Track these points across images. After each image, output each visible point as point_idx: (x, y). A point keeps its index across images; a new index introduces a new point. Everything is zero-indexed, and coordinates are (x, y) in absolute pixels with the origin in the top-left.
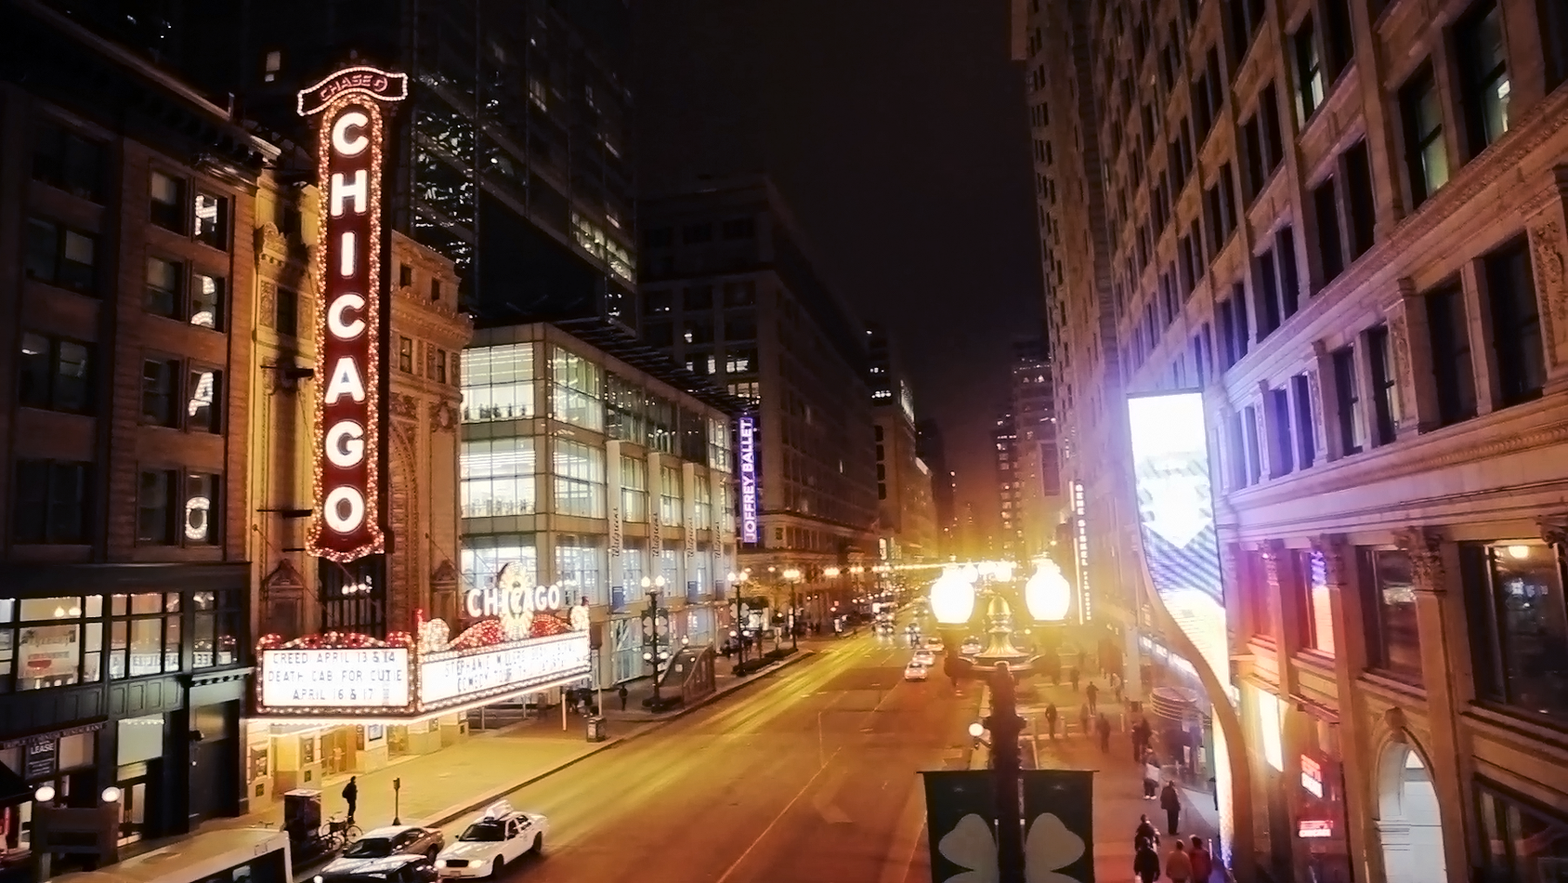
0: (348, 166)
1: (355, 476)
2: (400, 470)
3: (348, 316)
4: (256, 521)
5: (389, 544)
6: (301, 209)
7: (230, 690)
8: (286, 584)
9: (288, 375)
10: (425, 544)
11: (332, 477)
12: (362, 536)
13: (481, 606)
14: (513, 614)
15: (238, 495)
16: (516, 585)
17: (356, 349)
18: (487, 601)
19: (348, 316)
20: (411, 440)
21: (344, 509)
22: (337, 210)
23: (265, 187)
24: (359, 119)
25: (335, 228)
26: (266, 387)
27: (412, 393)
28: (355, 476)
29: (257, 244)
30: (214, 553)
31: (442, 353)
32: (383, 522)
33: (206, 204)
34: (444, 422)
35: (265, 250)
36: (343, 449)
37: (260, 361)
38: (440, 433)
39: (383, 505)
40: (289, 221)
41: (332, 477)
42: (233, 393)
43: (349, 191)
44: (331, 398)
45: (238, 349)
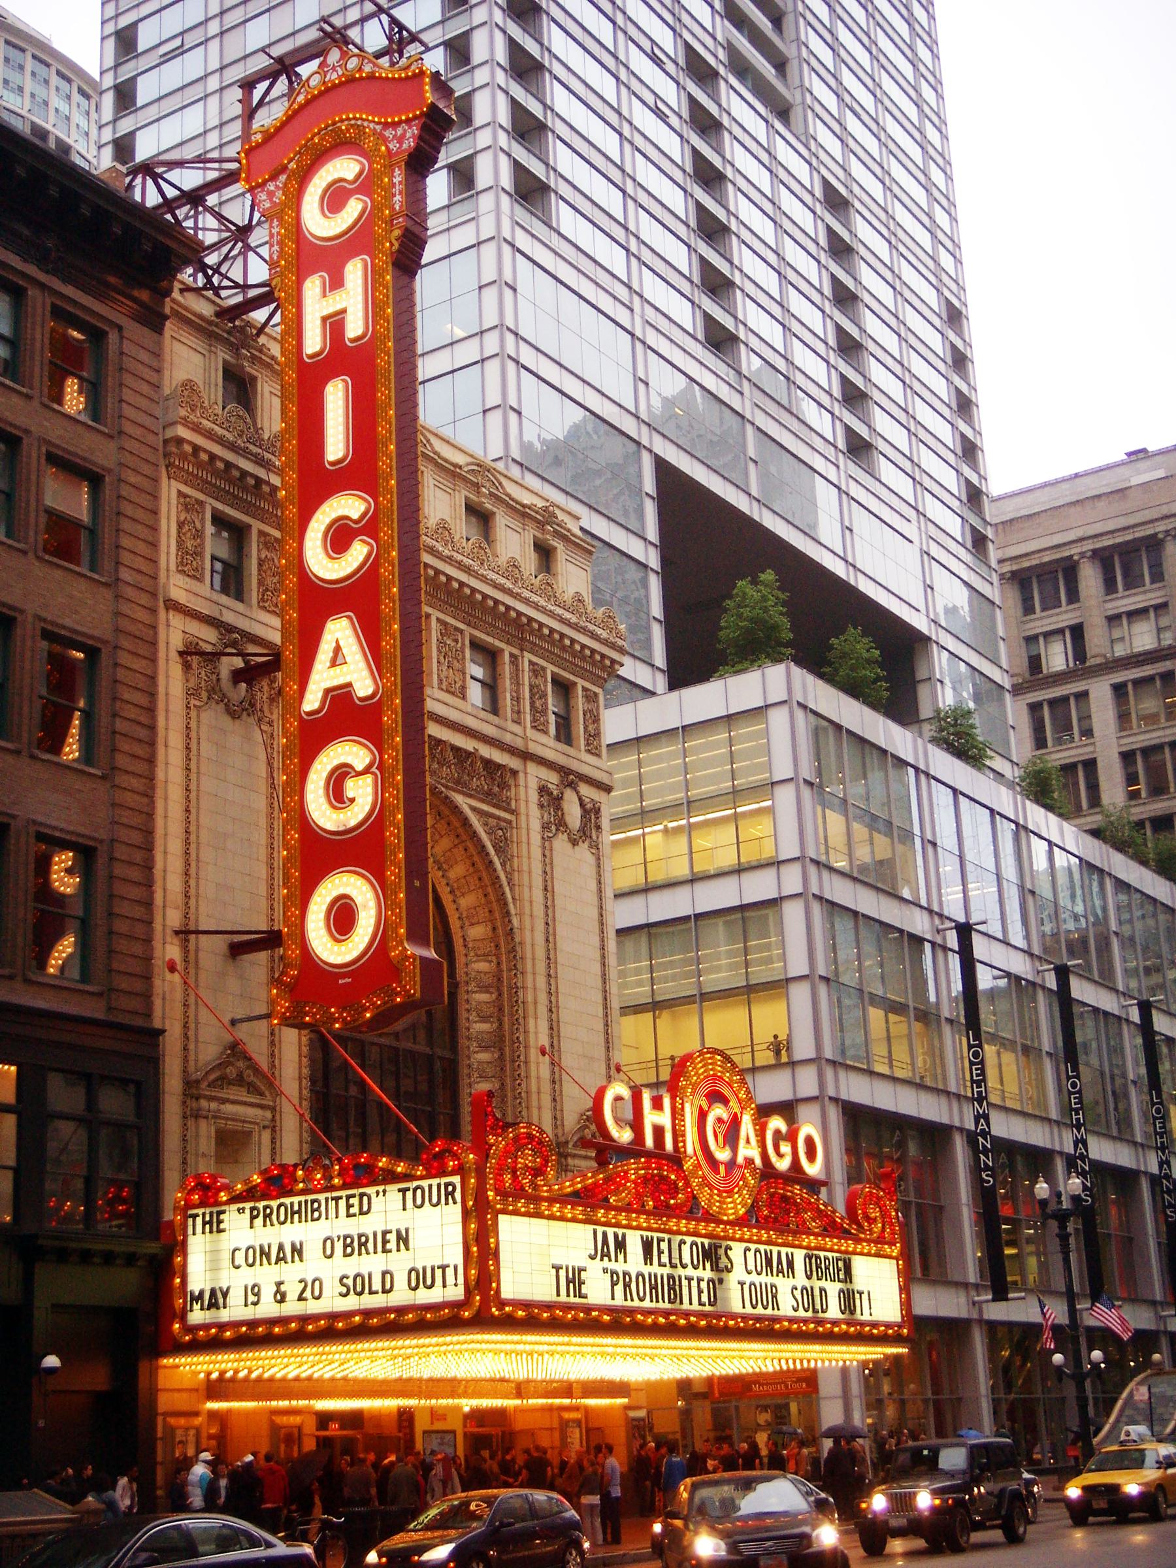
1: (358, 849)
3: (340, 537)
10: (540, 1068)
11: (318, 854)
12: (377, 965)
13: (637, 1125)
16: (716, 1097)
17: (356, 597)
18: (651, 1118)
19: (340, 537)
21: (342, 918)
22: (313, 341)
24: (345, 168)
36: (337, 794)
41: (318, 854)
44: (312, 701)
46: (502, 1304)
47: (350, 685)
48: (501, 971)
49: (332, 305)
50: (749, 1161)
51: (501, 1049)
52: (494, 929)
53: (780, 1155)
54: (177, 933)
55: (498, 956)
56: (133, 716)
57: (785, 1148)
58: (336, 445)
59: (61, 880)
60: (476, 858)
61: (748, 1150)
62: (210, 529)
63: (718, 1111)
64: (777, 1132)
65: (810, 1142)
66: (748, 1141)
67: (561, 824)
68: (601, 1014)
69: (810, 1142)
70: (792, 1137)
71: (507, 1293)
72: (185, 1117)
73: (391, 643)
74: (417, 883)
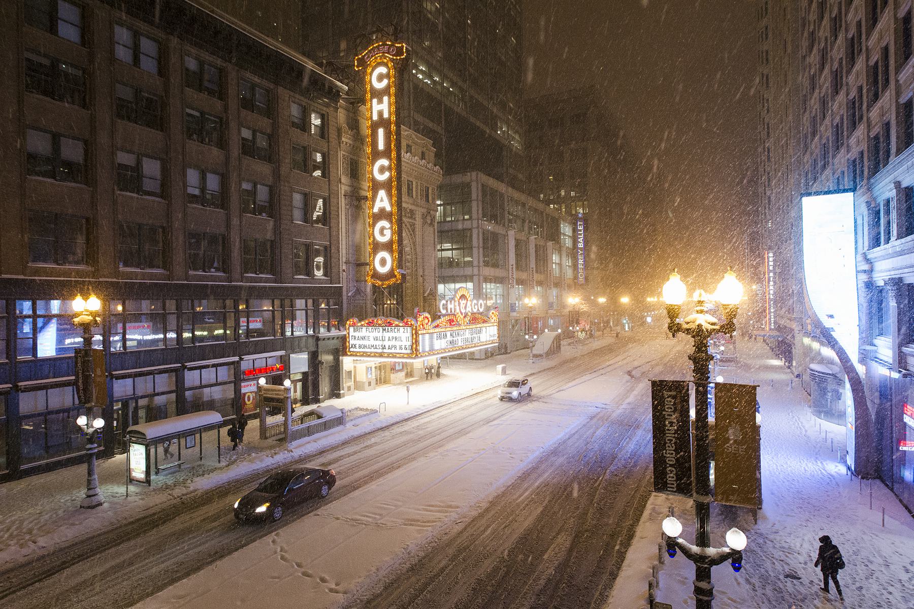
0: (378, 94)
3: (382, 170)
4: (344, 267)
9: (357, 200)
12: (391, 274)
13: (447, 309)
18: (449, 306)
19: (382, 170)
20: (414, 230)
22: (375, 117)
25: (374, 127)
27: (413, 207)
28: (388, 246)
37: (343, 192)
40: (354, 124)
43: (380, 107)
44: (376, 210)
45: (333, 187)
58: (381, 146)
73: (394, 199)
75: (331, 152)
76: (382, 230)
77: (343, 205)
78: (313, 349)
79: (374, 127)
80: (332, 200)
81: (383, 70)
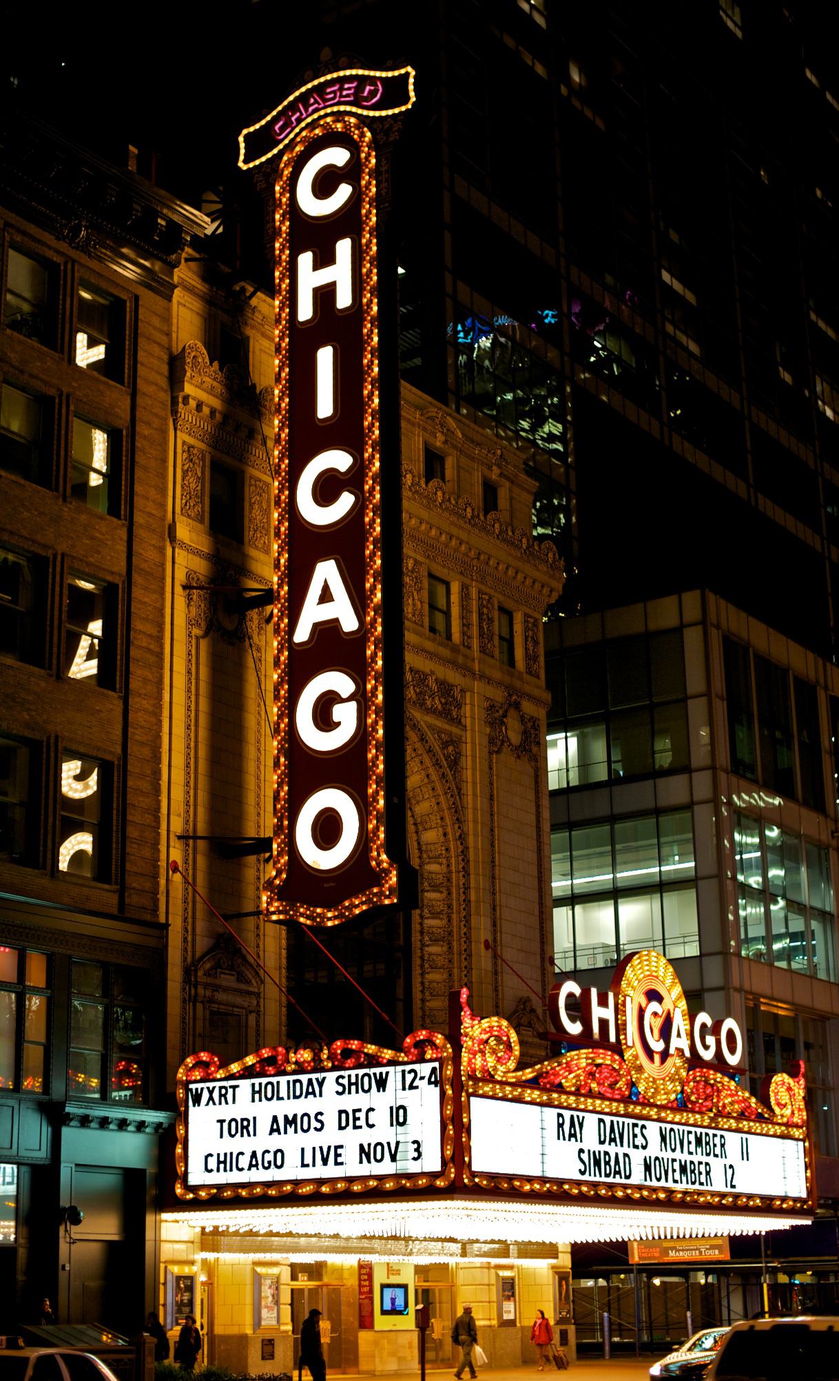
1: (343, 769)
2: (435, 819)
3: (326, 490)
4: (176, 855)
5: (410, 882)
6: (249, 332)
7: (130, 1150)
8: (228, 980)
9: (229, 606)
11: (306, 771)
12: (357, 872)
14: (649, 1053)
15: (144, 802)
16: (653, 996)
18: (597, 1012)
20: (455, 763)
21: (327, 829)
22: (305, 311)
23: (189, 289)
26: (190, 623)
27: (453, 677)
29: (175, 378)
30: (106, 897)
31: (508, 614)
32: (396, 846)
33: (92, 344)
34: (515, 738)
35: (189, 389)
36: (324, 720)
37: (181, 576)
38: (507, 757)
39: (396, 818)
41: (306, 771)
42: (137, 624)
43: (324, 276)
44: (302, 634)
45: (145, 552)
46: (474, 1175)
47: (336, 620)
48: (450, 872)
49: (324, 276)
50: (680, 1051)
51: (449, 943)
52: (445, 834)
53: (706, 1047)
54: (179, 838)
55: (448, 859)
56: (144, 644)
57: (711, 1040)
59: (69, 785)
60: (431, 771)
61: (679, 1042)
62: (496, 614)
63: (654, 1006)
64: (704, 1026)
65: (731, 1034)
66: (679, 1035)
67: (505, 740)
68: (537, 913)
69: (731, 1034)
70: (716, 1030)
71: (476, 1167)
72: (184, 1001)
74: (396, 800)
75: (142, 429)
76: (328, 701)
77: (180, 620)
78: (41, 1154)
79: (301, 345)
80: (137, 592)
81: (337, 156)
